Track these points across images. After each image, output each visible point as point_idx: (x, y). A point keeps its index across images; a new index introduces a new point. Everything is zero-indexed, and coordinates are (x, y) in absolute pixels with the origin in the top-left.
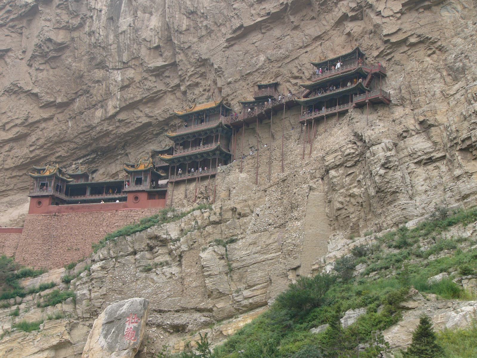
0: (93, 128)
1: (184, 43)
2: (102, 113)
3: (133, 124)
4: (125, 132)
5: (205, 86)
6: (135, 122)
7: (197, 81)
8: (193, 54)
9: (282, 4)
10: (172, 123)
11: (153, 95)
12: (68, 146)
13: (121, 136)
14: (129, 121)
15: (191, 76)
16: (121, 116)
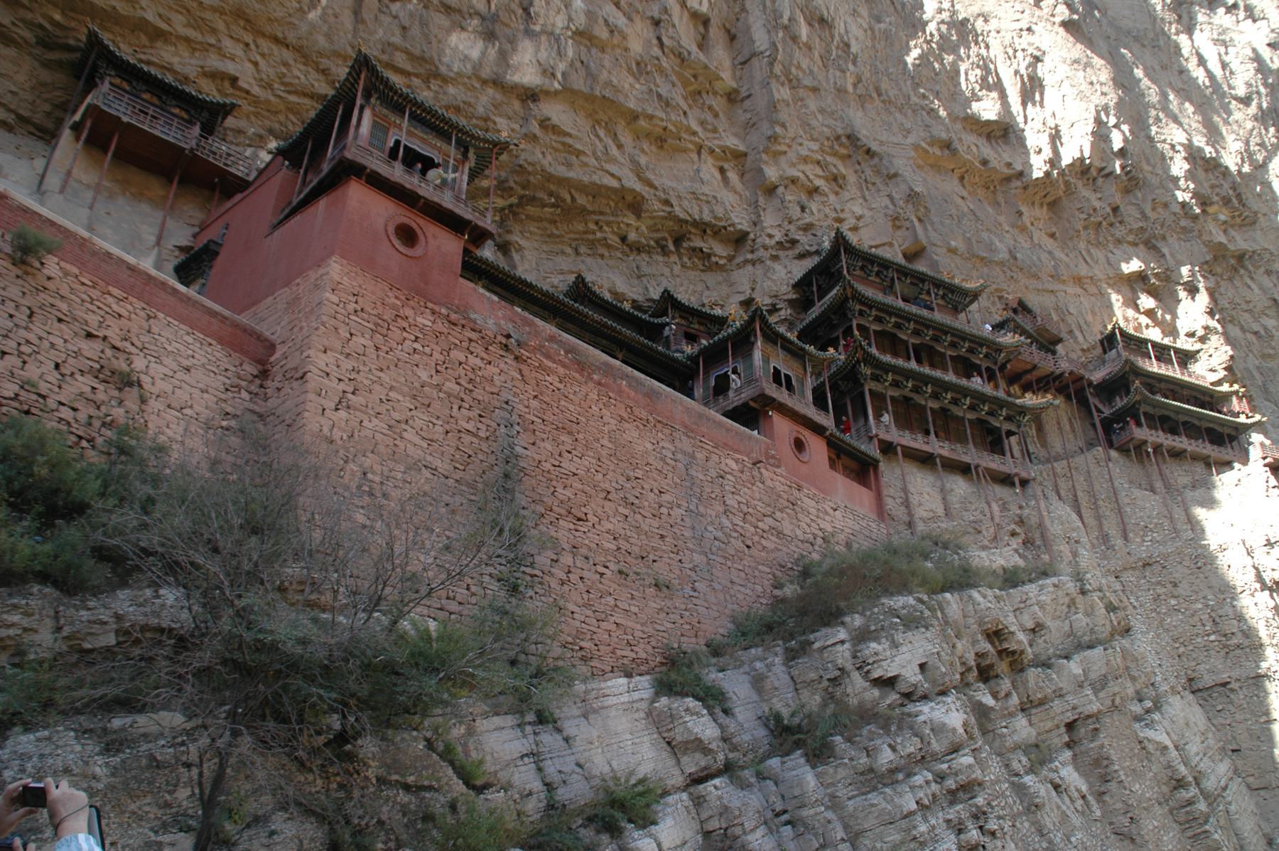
0: (433, 75)
1: (799, 67)
2: (483, 53)
3: (586, 165)
4: (551, 170)
5: (842, 211)
6: (593, 162)
7: (819, 182)
8: (822, 111)
9: (1009, 165)
10: (698, 243)
11: (671, 127)
12: (286, 64)
13: (529, 173)
14: (578, 146)
15: (805, 160)
16: (556, 112)
